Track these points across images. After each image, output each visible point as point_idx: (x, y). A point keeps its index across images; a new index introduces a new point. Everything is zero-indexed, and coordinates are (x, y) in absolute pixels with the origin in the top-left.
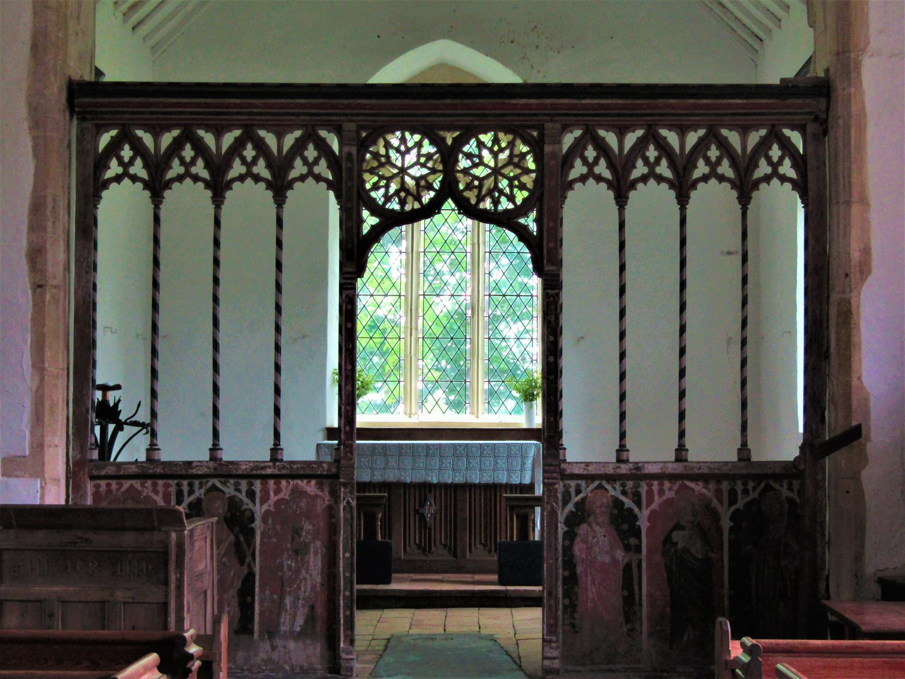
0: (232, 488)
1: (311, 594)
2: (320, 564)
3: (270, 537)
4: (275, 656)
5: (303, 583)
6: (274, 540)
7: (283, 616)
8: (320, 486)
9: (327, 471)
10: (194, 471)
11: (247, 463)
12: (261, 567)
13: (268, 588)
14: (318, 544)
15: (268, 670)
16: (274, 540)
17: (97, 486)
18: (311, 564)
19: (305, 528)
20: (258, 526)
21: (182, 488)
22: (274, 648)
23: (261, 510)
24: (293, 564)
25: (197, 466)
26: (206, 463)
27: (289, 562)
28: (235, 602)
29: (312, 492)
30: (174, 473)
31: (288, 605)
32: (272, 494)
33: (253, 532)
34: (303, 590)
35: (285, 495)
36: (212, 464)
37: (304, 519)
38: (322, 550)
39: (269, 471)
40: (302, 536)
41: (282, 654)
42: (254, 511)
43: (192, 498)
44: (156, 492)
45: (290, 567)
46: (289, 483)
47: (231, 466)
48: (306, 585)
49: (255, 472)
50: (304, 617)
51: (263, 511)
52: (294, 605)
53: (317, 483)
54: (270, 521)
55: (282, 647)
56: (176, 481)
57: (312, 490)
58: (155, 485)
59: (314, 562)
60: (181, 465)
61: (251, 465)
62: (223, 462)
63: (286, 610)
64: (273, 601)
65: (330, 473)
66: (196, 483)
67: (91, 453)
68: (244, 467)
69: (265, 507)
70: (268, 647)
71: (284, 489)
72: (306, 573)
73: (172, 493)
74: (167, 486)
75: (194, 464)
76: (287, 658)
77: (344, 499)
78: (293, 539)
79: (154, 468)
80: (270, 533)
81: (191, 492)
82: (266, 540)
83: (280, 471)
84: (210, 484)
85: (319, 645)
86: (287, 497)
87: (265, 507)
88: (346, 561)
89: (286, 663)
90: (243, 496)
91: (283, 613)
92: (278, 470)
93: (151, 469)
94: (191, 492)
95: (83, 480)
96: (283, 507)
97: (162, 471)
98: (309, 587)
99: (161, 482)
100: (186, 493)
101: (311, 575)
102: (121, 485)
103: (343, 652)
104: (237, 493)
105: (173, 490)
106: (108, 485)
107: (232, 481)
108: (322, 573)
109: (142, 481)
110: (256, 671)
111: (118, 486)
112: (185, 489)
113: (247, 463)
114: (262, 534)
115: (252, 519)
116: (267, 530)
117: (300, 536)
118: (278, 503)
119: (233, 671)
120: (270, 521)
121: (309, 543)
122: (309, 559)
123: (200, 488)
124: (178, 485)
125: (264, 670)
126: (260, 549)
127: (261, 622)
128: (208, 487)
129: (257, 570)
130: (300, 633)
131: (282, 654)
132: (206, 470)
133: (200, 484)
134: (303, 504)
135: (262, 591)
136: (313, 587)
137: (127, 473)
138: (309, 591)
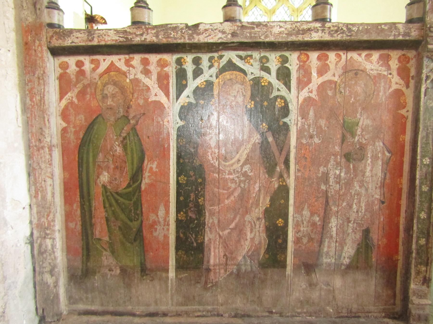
0: (257, 65)
1: (365, 215)
2: (380, 174)
3: (311, 137)
4: (315, 295)
5: (355, 201)
6: (316, 140)
7: (326, 244)
8: (385, 59)
9: (403, 36)
10: (202, 39)
11: (282, 24)
12: (297, 178)
13: (306, 207)
14: (379, 144)
15: (305, 313)
16: (316, 140)
17: (64, 66)
18: (368, 174)
19: (360, 124)
20: (293, 122)
21: (184, 67)
22: (312, 285)
23: (298, 97)
24: (342, 174)
25: (206, 30)
26: (219, 25)
27: (338, 172)
28: (261, 226)
29: (372, 70)
30: (171, 41)
31: (334, 229)
32: (314, 74)
33: (286, 128)
34: (355, 210)
35: (334, 75)
36: (228, 26)
37: (359, 110)
38: (384, 154)
39: (315, 37)
40: (356, 135)
41: (323, 293)
42: (288, 100)
43: (200, 81)
44: (147, 72)
45: (338, 178)
46: (339, 56)
47: (256, 29)
48: (359, 202)
49: (293, 38)
50: (355, 246)
51: (301, 99)
52: (342, 230)
53: (381, 57)
54: (311, 113)
55: (324, 285)
56: (175, 57)
57: (373, 67)
58: (145, 62)
59: (371, 171)
60: (182, 29)
61: (288, 26)
62: (244, 24)
63: (331, 237)
64: (314, 224)
65: (407, 38)
66: (205, 58)
67: (49, 14)
68: (276, 30)
69: (304, 93)
70: (304, 285)
71: (332, 66)
72: (360, 187)
73: (170, 74)
74: (162, 64)
75: (201, 27)
76: (331, 297)
77: (427, 77)
78: (343, 139)
79: (142, 35)
80: (311, 131)
81: (197, 73)
82: (304, 141)
83: (332, 36)
84: (224, 61)
85: (373, 282)
86: (336, 79)
87: (304, 93)
88: (424, 170)
89: (328, 304)
90: (272, 78)
91: (327, 240)
92: (329, 33)
93: (137, 35)
94: (197, 73)
95: (40, 55)
96: (330, 93)
97: (154, 39)
98: (363, 205)
99: (154, 58)
100: (190, 74)
101: (367, 190)
102: (97, 64)
103: (414, 293)
104: (263, 74)
105: (171, 70)
106: (79, 64)
107: (256, 55)
108: (383, 185)
109: (127, 57)
110: (289, 314)
111: (93, 66)
112: (189, 67)
113: (282, 24)
114: (300, 133)
115: (285, 111)
116: (306, 127)
117: (353, 135)
118: (322, 88)
119: (260, 314)
120: (311, 113)
121: (366, 145)
122: (365, 166)
123: (210, 67)
124: (179, 62)
125: (299, 313)
126: (297, 153)
127: (296, 253)
128: (221, 66)
129: (291, 182)
130: (349, 267)
131: (323, 293)
132: (220, 35)
133: (211, 59)
134: (359, 89)
135: (299, 209)
136: (369, 205)
137: (103, 43)
138: (363, 211)
